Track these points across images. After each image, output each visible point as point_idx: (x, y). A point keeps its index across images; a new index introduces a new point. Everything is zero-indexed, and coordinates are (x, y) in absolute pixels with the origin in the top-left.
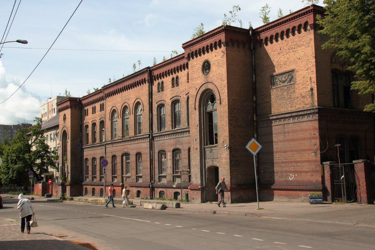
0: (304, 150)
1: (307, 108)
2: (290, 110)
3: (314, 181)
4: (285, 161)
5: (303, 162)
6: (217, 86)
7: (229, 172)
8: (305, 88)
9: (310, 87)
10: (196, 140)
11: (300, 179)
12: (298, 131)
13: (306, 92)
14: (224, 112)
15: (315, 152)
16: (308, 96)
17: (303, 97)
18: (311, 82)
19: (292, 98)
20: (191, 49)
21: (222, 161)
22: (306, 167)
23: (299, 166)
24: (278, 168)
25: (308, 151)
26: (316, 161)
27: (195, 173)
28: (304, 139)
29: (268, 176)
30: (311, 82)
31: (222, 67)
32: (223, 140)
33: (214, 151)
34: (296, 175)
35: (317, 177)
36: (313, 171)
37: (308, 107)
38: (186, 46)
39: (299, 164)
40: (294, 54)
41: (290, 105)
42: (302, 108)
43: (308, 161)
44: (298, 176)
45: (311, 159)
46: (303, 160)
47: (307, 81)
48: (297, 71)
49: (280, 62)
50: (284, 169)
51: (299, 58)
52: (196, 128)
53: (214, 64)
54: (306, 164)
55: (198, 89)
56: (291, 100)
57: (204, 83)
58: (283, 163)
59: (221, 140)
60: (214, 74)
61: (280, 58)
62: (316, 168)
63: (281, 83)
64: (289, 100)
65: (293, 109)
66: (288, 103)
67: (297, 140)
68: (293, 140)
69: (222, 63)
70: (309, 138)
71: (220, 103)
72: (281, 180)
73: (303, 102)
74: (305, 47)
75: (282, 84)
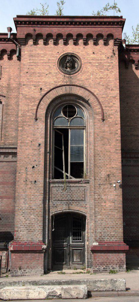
6: (95, 94)
10: (33, 167)
14: (111, 133)
20: (37, 29)
21: (103, 204)
27: (28, 222)
31: (108, 70)
33: (72, 189)
38: (19, 21)
52: (36, 147)
53: (90, 63)
55: (46, 90)
57: (63, 84)
59: (103, 173)
60: (89, 76)
69: (110, 66)
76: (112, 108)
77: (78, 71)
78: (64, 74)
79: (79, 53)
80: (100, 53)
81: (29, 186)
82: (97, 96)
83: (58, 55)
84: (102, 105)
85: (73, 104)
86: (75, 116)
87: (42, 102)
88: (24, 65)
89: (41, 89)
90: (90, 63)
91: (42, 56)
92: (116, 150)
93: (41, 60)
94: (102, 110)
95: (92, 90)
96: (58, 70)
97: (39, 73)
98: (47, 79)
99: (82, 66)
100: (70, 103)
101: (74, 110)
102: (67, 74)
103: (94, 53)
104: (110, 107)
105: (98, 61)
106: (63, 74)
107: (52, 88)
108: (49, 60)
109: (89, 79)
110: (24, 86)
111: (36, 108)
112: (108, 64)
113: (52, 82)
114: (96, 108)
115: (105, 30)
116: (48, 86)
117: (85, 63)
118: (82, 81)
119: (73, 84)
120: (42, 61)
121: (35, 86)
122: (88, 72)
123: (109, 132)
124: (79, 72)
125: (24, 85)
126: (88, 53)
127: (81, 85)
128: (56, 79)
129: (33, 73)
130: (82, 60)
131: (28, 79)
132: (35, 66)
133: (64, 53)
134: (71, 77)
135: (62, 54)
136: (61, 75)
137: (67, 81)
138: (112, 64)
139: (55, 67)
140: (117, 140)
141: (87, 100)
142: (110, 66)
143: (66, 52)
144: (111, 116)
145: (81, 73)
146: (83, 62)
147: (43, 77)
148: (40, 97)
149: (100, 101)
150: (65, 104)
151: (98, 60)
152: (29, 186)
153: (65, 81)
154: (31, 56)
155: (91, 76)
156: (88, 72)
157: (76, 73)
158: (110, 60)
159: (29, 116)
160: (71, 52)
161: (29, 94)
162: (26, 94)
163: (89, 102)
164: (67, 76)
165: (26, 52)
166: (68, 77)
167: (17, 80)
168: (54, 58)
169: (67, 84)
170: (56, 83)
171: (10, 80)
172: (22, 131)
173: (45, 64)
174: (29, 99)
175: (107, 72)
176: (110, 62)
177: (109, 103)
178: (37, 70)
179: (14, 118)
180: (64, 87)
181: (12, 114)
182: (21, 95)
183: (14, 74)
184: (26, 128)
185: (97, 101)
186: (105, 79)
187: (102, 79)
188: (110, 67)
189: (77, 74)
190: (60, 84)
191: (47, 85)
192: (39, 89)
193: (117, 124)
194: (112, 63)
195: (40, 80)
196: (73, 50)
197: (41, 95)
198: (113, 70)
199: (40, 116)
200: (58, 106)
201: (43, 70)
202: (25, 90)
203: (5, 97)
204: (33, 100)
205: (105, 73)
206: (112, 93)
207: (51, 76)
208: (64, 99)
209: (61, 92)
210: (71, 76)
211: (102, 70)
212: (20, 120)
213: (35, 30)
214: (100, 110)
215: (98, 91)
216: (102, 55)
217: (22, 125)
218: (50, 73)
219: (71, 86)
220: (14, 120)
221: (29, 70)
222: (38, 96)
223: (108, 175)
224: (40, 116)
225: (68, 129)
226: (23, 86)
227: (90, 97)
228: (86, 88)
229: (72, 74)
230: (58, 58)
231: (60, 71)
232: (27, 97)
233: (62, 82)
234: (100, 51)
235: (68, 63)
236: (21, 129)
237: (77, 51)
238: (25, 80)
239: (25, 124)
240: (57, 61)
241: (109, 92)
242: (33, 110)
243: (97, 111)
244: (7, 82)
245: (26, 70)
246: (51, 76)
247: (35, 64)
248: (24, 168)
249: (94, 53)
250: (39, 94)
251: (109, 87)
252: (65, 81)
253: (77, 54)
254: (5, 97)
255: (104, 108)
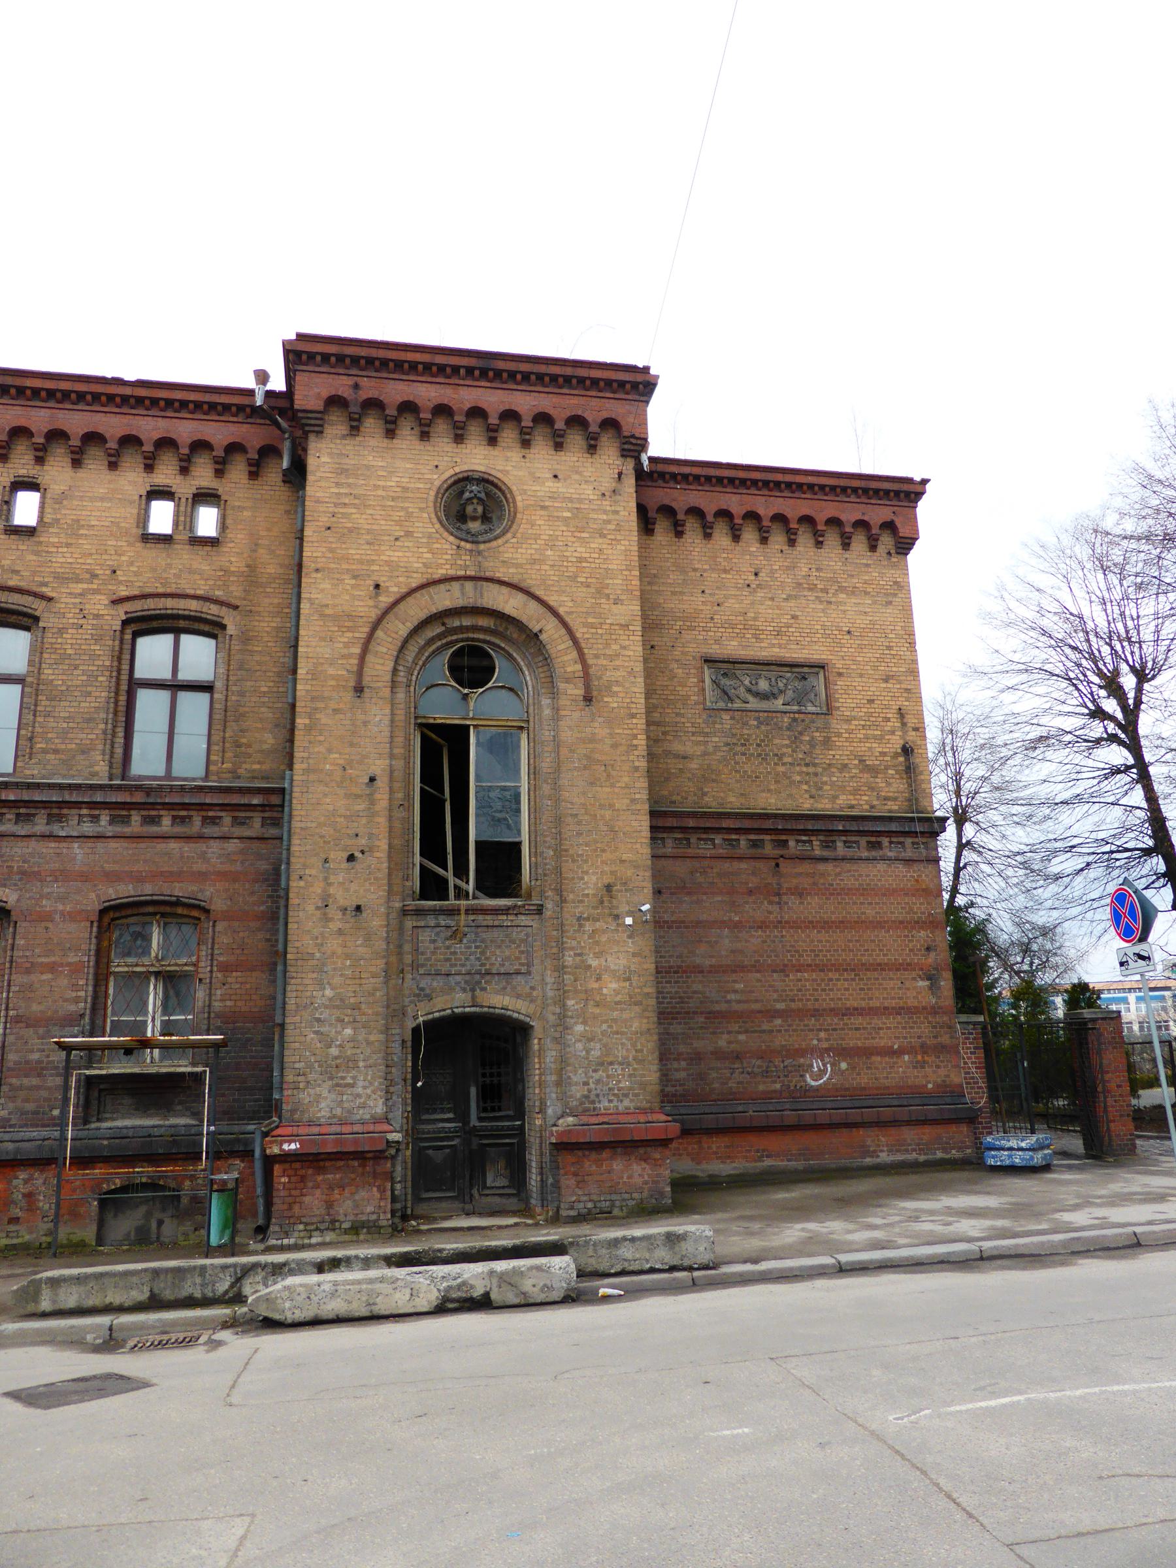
0: (880, 967)
1: (890, 811)
2: (806, 805)
3: (930, 1086)
4: (780, 1006)
5: (872, 1011)
6: (561, 611)
7: (649, 1046)
8: (880, 739)
9: (902, 742)
10: (351, 858)
11: (863, 1079)
12: (848, 891)
13: (883, 754)
14: (615, 746)
15: (929, 978)
16: (890, 772)
17: (873, 771)
18: (904, 724)
19: (815, 765)
20: (364, 382)
22: (889, 1033)
23: (856, 1029)
24: (742, 1037)
25: (898, 970)
26: (934, 1011)
28: (879, 925)
29: (683, 1074)
30: (904, 724)
32: (607, 880)
34: (844, 1066)
35: (942, 1072)
36: (924, 1049)
37: (893, 807)
38: (303, 353)
39: (858, 1021)
40: (823, 611)
41: (805, 787)
42: (867, 807)
43: (898, 1011)
44: (852, 1067)
45: (912, 1002)
46: (875, 1003)
47: (888, 720)
48: (840, 674)
49: (755, 619)
50: (779, 1041)
51: (849, 632)
53: (543, 508)
54: (891, 1021)
55: (394, 590)
56: (811, 770)
57: (452, 572)
58: (772, 1014)
61: (753, 603)
62: (935, 1037)
63: (751, 698)
64: (804, 769)
65: (820, 806)
66: (798, 778)
67: (842, 924)
68: (825, 925)
69: (609, 522)
70: (901, 922)
71: (588, 699)
72: (761, 1088)
73: (872, 789)
74: (875, 603)
75: (754, 703)
76: (617, 663)
77: (504, 533)
78: (457, 542)
79: (507, 472)
80: (576, 477)
81: (334, 926)
82: (567, 619)
83: (435, 477)
84: (586, 651)
85: (484, 641)
86: (490, 685)
87: (379, 633)
88: (318, 502)
89: (377, 586)
90: (543, 508)
91: (380, 473)
92: (633, 801)
93: (376, 487)
94: (585, 666)
95: (552, 600)
96: (438, 526)
97: (369, 532)
98: (397, 554)
99: (519, 516)
100: (473, 640)
101: (485, 663)
102: (467, 541)
103: (555, 476)
104: (611, 658)
105: (570, 505)
106: (451, 539)
107: (414, 585)
108: (406, 489)
109: (541, 561)
110: (319, 575)
111: (357, 650)
112: (605, 517)
113: (416, 565)
114: (565, 658)
115: (595, 408)
116: (401, 579)
117: (527, 507)
118: (517, 566)
119: (488, 574)
120: (380, 492)
121: (355, 577)
122: (537, 537)
123: (608, 741)
124: (509, 535)
125: (317, 570)
126: (538, 475)
127: (515, 580)
128: (429, 556)
129: (351, 530)
130: (519, 498)
131: (331, 550)
132: (355, 506)
133: (457, 470)
134: (479, 553)
135: (451, 472)
136: (446, 544)
137: (466, 564)
138: (617, 517)
139: (425, 515)
140: (636, 769)
141: (536, 630)
142: (609, 522)
143: (466, 468)
144: (615, 689)
145: (514, 540)
146: (519, 504)
147: (383, 548)
148: (374, 614)
149: (578, 635)
150: (457, 641)
151: (571, 500)
152: (334, 926)
153: (459, 562)
154: (342, 471)
155: (549, 553)
156: (537, 537)
157: (496, 538)
158: (608, 503)
159: (333, 677)
160: (482, 469)
161: (336, 601)
162: (325, 602)
163: (543, 637)
164: (468, 546)
165: (324, 459)
166: (471, 551)
167: (283, 553)
168: (421, 486)
169: (468, 573)
170: (430, 571)
171: (255, 551)
172: (309, 729)
173: (392, 504)
174: (335, 618)
175: (601, 541)
176: (608, 508)
177: (607, 645)
178: (362, 521)
179: (271, 684)
180: (456, 586)
181: (264, 668)
182: (308, 605)
183: (269, 530)
184: (324, 721)
185: (567, 637)
186: (593, 565)
187: (584, 564)
188: (609, 527)
189: (500, 541)
190: (444, 572)
191: (396, 574)
192: (371, 588)
193: (633, 716)
194: (617, 512)
195: (374, 558)
196: (486, 462)
197: (376, 607)
198: (619, 537)
199: (375, 679)
200: (434, 647)
201: (383, 522)
202: (322, 586)
203: (236, 607)
204: (350, 624)
205: (592, 545)
206: (616, 611)
207: (410, 544)
208: (457, 623)
209: (445, 598)
210: (482, 547)
211: (583, 535)
212: (303, 693)
213: (356, 386)
214: (579, 667)
215: (570, 604)
216: (583, 486)
217: (308, 710)
218: (409, 534)
219: (480, 583)
220: (268, 692)
221: (334, 519)
222: (367, 610)
223: (609, 888)
224: (375, 679)
225: (469, 726)
226: (314, 575)
227: (543, 622)
228: (532, 590)
229: (484, 542)
230: (437, 483)
231: (442, 530)
232: (328, 611)
233: (448, 567)
234: (577, 472)
235: (474, 506)
236: (307, 721)
237: (501, 468)
238: (320, 554)
239: (321, 705)
240: (432, 493)
241: (607, 607)
242: (350, 656)
243: (569, 669)
244: (245, 555)
245: (325, 520)
246: (410, 544)
247: (357, 501)
248: (316, 862)
249: (555, 476)
250: (371, 603)
251: (607, 591)
252: (459, 562)
253: (499, 475)
254: (236, 607)
255: (590, 662)
